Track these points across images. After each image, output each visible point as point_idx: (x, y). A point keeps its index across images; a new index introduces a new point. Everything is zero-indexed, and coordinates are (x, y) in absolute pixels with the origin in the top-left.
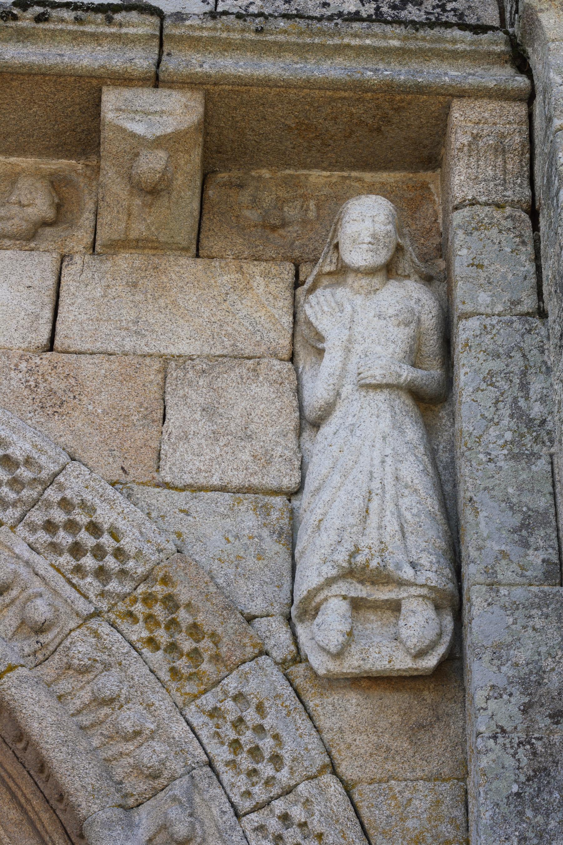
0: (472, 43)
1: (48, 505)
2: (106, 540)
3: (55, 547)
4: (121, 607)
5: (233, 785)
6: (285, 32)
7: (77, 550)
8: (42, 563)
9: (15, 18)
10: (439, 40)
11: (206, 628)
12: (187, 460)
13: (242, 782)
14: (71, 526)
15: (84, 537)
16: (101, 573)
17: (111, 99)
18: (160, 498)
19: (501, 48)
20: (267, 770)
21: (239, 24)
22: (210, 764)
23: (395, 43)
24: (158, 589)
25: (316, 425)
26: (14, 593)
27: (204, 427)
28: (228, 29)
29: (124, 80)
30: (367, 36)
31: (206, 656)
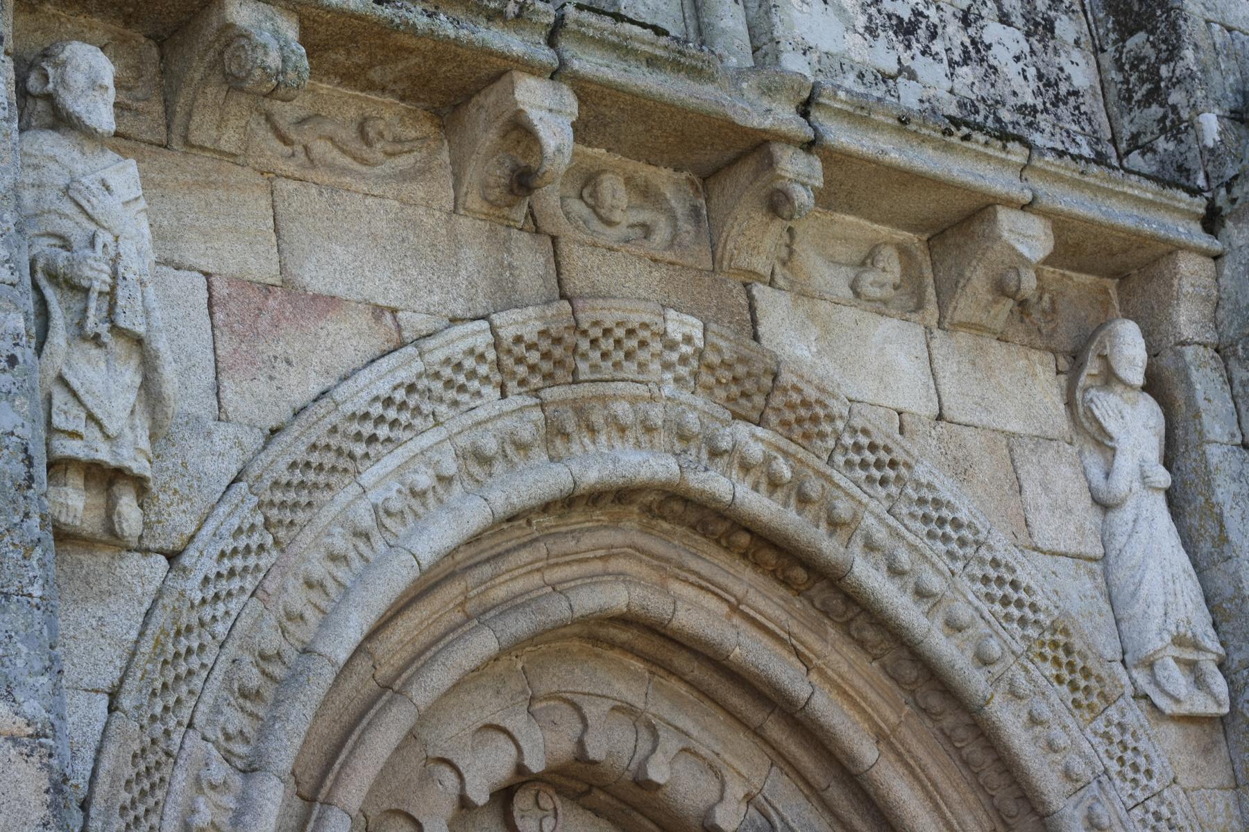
0: (1188, 204)
1: (982, 561)
2: (1023, 595)
3: (990, 598)
5: (1122, 789)
6: (1096, 176)
7: (1005, 601)
8: (985, 607)
9: (951, 134)
10: (1173, 198)
11: (1094, 672)
13: (1128, 785)
15: (1008, 589)
16: (1023, 621)
19: (1202, 211)
21: (1072, 165)
22: (1106, 772)
23: (1150, 196)
26: (970, 631)
27: (1043, 500)
28: (1067, 168)
29: (1009, 203)
30: (1138, 187)
31: (1096, 693)
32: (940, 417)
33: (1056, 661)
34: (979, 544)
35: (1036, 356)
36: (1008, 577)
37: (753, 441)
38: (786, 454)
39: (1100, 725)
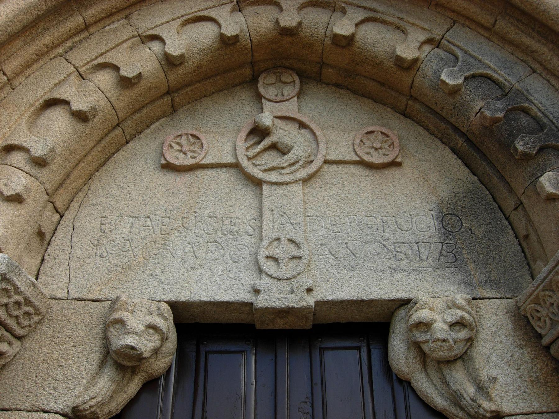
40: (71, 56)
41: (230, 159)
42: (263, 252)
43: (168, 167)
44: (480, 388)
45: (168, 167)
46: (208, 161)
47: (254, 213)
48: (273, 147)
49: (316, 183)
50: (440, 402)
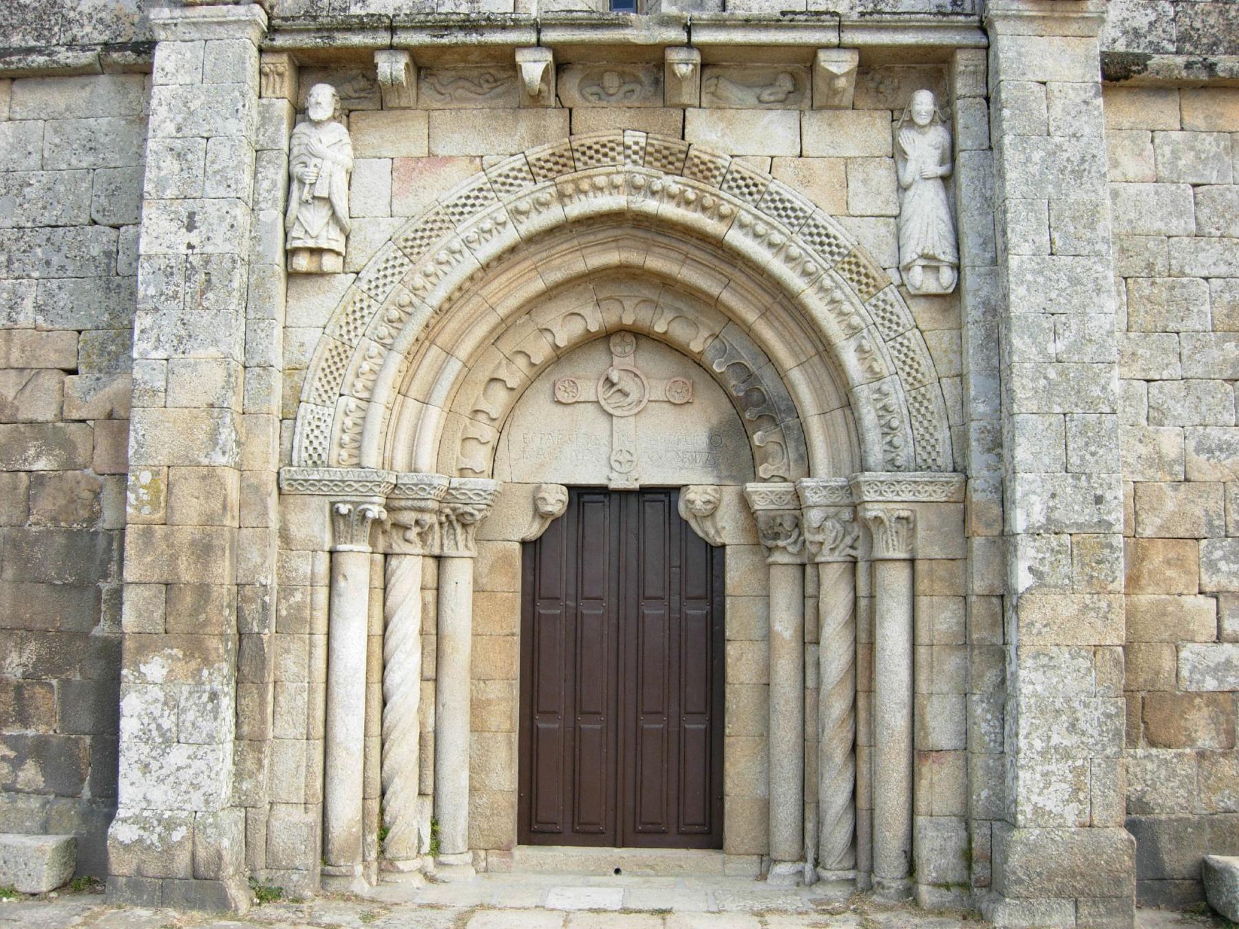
1: (809, 226)
3: (813, 243)
4: (840, 266)
7: (821, 244)
8: (809, 248)
12: (857, 207)
13: (886, 331)
14: (819, 235)
15: (824, 238)
16: (832, 253)
17: (822, 55)
18: (849, 222)
20: (895, 327)
24: (853, 260)
25: (905, 190)
29: (827, 47)
32: (801, 156)
33: (850, 271)
34: (806, 218)
35: (877, 114)
36: (823, 232)
37: (672, 183)
38: (693, 188)
39: (873, 301)
40: (499, 343)
41: (593, 399)
42: (613, 458)
43: (559, 402)
44: (717, 532)
45: (559, 402)
46: (581, 399)
47: (608, 433)
48: (619, 391)
49: (643, 415)
50: (701, 534)
